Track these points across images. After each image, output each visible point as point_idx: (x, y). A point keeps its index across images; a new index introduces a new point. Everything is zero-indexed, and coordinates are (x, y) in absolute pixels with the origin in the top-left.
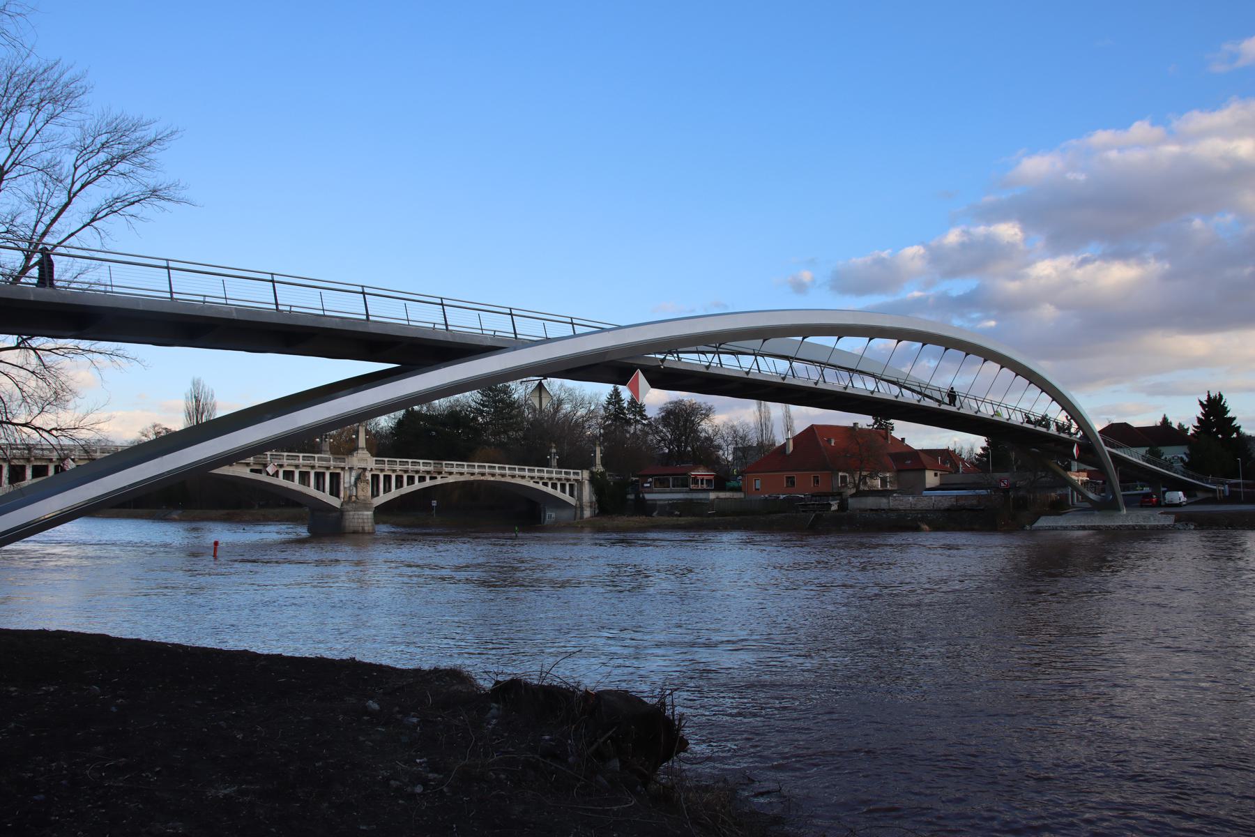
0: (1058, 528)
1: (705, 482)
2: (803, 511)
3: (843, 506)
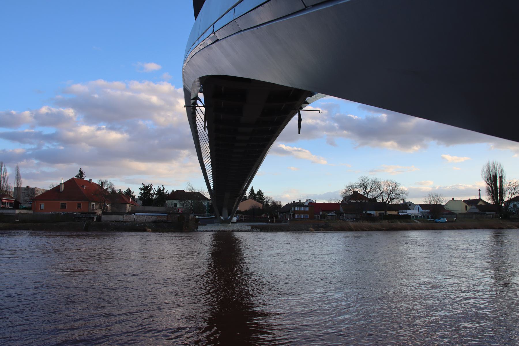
0: (209, 231)
1: (9, 203)
2: (78, 221)
3: (99, 218)
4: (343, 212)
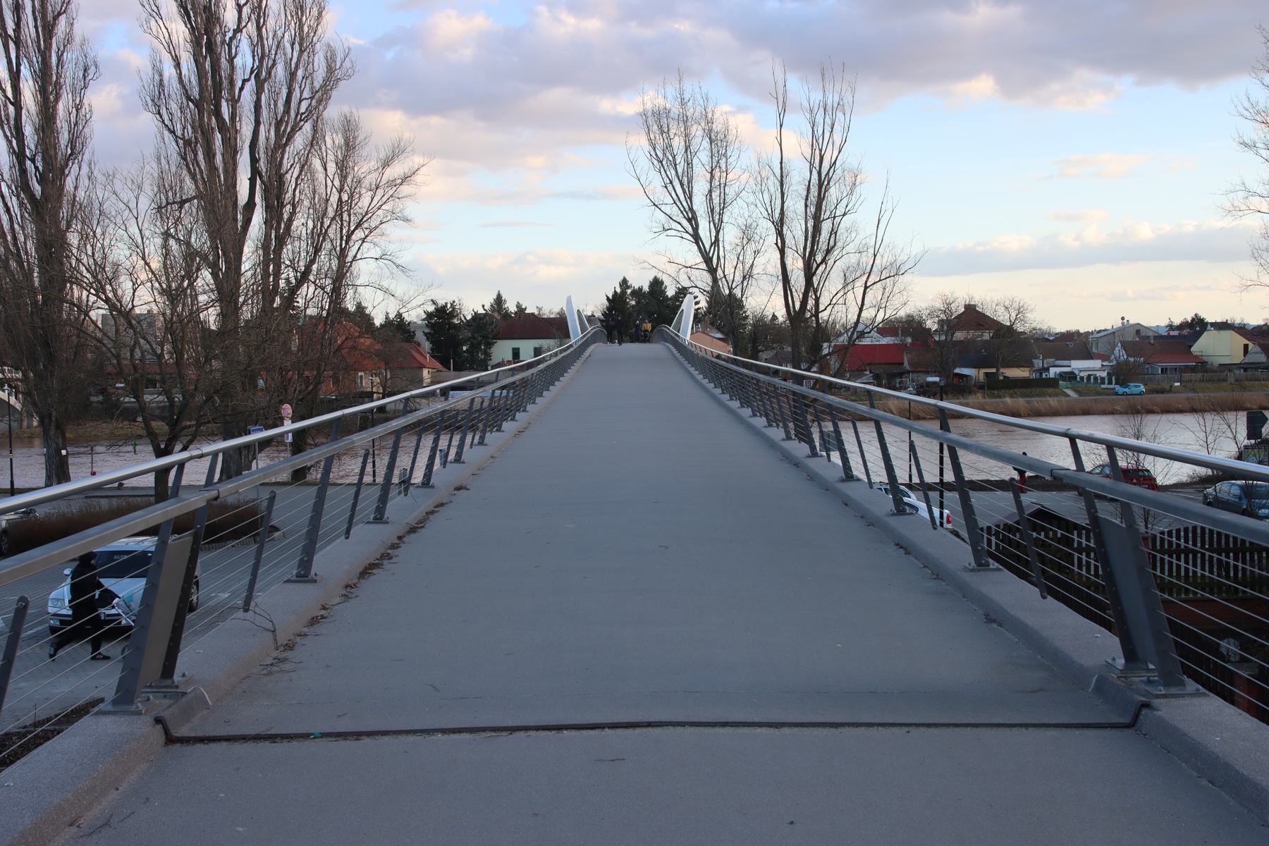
4: (909, 369)
